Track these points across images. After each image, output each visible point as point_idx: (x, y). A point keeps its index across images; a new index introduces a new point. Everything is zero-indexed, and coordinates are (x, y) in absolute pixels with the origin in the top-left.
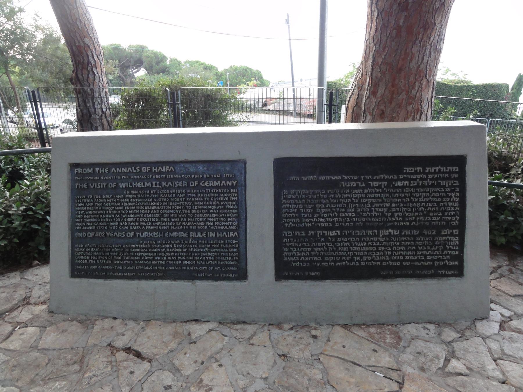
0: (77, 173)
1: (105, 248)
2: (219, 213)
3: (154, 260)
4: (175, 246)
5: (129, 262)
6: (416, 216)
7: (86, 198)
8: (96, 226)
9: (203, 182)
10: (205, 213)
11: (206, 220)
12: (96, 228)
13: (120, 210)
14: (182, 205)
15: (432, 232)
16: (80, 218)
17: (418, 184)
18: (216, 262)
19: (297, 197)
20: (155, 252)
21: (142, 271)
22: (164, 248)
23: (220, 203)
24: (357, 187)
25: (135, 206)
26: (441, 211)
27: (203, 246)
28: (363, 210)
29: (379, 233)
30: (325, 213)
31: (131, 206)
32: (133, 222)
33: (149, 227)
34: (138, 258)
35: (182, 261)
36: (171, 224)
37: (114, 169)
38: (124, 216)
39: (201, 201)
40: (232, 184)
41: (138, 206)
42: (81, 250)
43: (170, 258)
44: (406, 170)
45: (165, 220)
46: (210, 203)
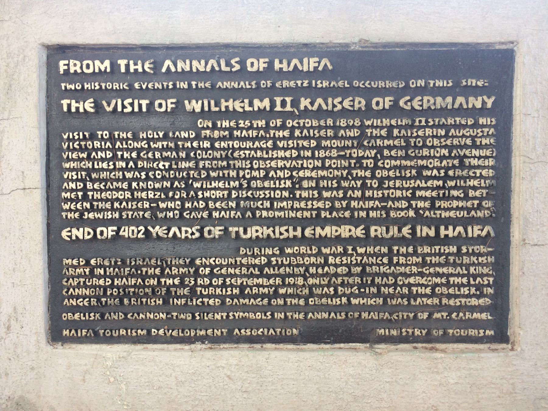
0: (67, 72)
1: (147, 266)
2: (447, 177)
3: (276, 294)
4: (331, 260)
5: (211, 302)
7: (93, 137)
9: (408, 98)
11: (413, 194)
12: (121, 216)
14: (351, 157)
16: (77, 190)
18: (436, 301)
21: (244, 323)
25: (227, 158)
27: (402, 260)
32: (222, 199)
33: (265, 214)
34: (236, 291)
36: (320, 205)
37: (168, 63)
38: (197, 185)
39: (401, 148)
41: (234, 159)
43: (318, 291)
45: (305, 194)
46: (425, 152)
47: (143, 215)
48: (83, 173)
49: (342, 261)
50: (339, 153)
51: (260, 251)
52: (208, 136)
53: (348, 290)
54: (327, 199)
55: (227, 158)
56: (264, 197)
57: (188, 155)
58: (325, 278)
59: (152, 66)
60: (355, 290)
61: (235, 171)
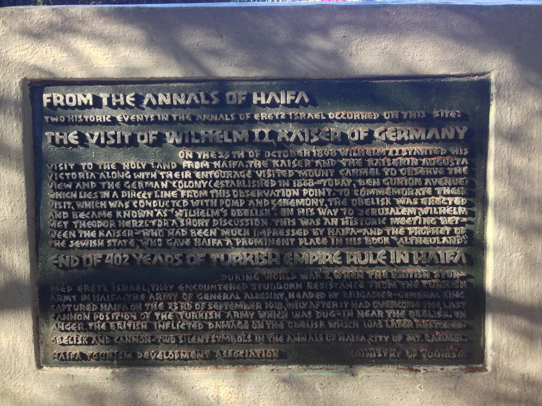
0: (50, 105)
1: (131, 292)
5: (194, 326)
8: (105, 239)
9: (382, 128)
13: (167, 198)
20: (259, 300)
22: (281, 291)
32: (203, 228)
35: (326, 320)
36: (299, 232)
39: (376, 177)
40: (456, 134)
42: (67, 298)
47: (127, 243)
48: (69, 203)
49: (320, 286)
50: (315, 183)
51: (241, 278)
52: (189, 167)
53: (325, 314)
54: (305, 227)
55: (208, 188)
56: (244, 225)
57: (170, 185)
58: (303, 303)
59: (133, 99)
60: (332, 314)
61: (216, 200)
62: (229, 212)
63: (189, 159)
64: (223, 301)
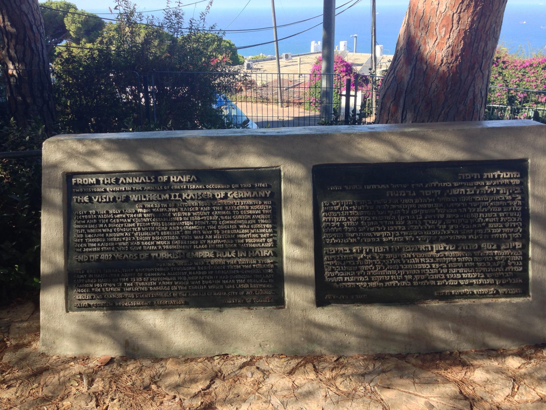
0: (76, 184)
3: (173, 284)
4: (199, 268)
6: (474, 229)
8: (101, 247)
9: (231, 192)
10: (234, 229)
11: (236, 236)
13: (131, 227)
14: (206, 220)
15: (492, 246)
17: (475, 192)
19: (339, 208)
23: (252, 217)
24: (407, 197)
26: (501, 222)
28: (414, 223)
29: (432, 248)
30: (372, 226)
31: (144, 222)
32: (148, 241)
33: (167, 247)
35: (207, 285)
36: (193, 242)
39: (229, 215)
40: (266, 195)
42: (82, 276)
44: (462, 176)
48: (84, 230)
55: (150, 222)
57: (132, 220)
60: (210, 282)
62: (160, 233)
63: (141, 208)
64: (157, 276)
